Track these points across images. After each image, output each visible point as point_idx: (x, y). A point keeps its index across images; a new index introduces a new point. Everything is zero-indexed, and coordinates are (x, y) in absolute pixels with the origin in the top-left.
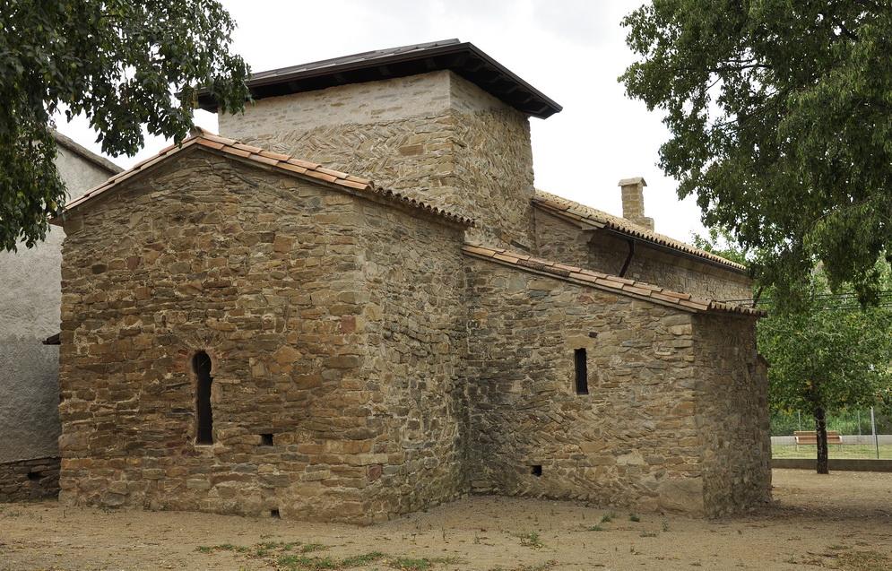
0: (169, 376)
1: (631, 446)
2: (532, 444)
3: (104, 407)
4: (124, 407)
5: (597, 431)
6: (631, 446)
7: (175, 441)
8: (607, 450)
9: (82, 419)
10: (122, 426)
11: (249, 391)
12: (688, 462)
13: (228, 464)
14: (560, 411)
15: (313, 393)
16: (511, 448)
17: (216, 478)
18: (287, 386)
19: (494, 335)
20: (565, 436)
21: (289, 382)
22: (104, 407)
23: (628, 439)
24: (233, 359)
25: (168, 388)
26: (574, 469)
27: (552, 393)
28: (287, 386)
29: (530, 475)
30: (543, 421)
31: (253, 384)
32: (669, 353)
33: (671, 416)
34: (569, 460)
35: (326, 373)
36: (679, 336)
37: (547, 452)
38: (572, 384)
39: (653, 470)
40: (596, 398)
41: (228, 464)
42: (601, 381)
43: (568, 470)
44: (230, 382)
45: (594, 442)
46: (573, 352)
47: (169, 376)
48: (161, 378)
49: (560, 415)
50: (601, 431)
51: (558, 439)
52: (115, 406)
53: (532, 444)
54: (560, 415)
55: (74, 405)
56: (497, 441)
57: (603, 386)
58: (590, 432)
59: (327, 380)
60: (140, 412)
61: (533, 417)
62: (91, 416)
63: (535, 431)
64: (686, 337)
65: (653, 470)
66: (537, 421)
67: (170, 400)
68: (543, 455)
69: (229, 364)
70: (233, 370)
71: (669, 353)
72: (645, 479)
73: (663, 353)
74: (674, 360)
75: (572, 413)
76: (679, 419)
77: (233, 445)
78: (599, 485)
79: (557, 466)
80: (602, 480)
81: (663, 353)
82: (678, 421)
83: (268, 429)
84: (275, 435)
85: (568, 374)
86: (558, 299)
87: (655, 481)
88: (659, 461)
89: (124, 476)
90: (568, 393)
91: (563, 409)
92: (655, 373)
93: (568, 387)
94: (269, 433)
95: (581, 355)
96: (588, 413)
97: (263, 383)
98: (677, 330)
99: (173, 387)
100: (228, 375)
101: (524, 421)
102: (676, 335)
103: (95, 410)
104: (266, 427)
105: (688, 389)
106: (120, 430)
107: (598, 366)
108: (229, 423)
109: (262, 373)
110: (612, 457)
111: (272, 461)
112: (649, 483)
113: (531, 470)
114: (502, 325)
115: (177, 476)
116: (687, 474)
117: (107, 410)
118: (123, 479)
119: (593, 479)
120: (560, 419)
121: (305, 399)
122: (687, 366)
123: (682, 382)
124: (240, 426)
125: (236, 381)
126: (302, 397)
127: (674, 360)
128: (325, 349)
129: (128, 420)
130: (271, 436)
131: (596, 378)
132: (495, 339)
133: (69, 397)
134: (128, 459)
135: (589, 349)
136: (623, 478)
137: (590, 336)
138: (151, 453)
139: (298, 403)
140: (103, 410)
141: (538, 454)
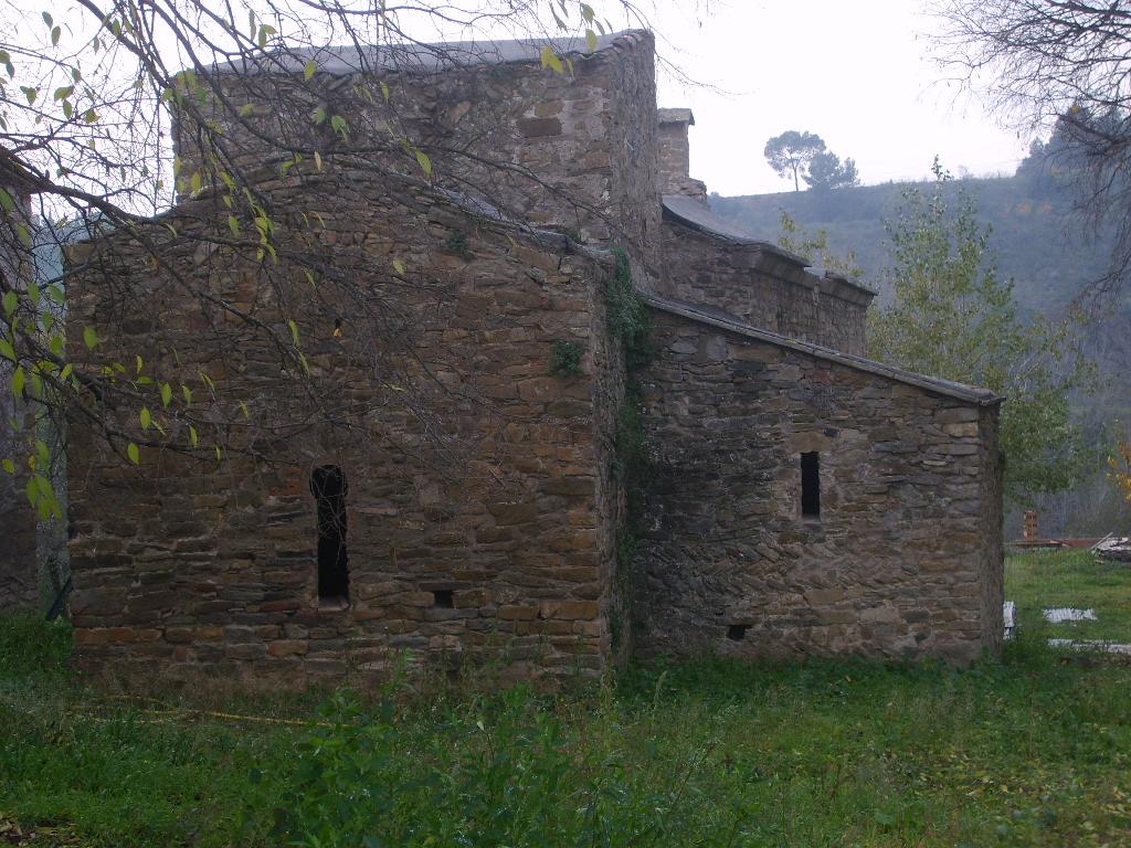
0: (272, 500)
1: (883, 596)
2: (730, 592)
3: (152, 547)
4: (190, 547)
5: (831, 575)
6: (883, 596)
7: (276, 605)
8: (845, 602)
9: (116, 566)
10: (187, 578)
11: (413, 526)
12: (964, 618)
13: (378, 637)
14: (776, 544)
15: (522, 531)
16: (697, 598)
17: (357, 657)
18: (479, 519)
19: (673, 426)
20: (781, 582)
21: (482, 514)
22: (152, 547)
23: (878, 585)
24: (387, 478)
25: (273, 519)
26: (794, 630)
27: (764, 517)
28: (479, 519)
29: (725, 639)
30: (749, 559)
31: (421, 516)
32: (943, 463)
33: (941, 552)
34: (788, 616)
35: (543, 501)
36: (958, 438)
37: (754, 604)
38: (797, 506)
39: (912, 630)
40: (832, 525)
41: (378, 637)
42: (842, 502)
43: (786, 632)
44: (382, 512)
45: (826, 590)
46: (799, 456)
47: (272, 500)
48: (256, 504)
49: (775, 549)
50: (838, 574)
51: (772, 586)
52: (174, 547)
53: (730, 592)
54: (775, 549)
55: (101, 545)
56: (676, 588)
57: (845, 508)
58: (821, 575)
59: (544, 512)
60: (220, 556)
61: (733, 554)
62: (129, 561)
63: (735, 574)
64: (969, 440)
65: (912, 630)
66: (739, 558)
67: (273, 538)
68: (748, 609)
69: (379, 484)
70: (386, 494)
71: (943, 463)
72: (899, 644)
73: (934, 463)
74: (950, 474)
75: (796, 547)
76: (953, 557)
77: (385, 607)
78: (833, 653)
79: (768, 625)
80: (837, 646)
81: (934, 463)
82: (952, 560)
83: (446, 584)
84: (460, 592)
85: (790, 491)
86: (777, 378)
87: (914, 644)
88: (920, 617)
89: (191, 653)
90: (791, 517)
91: (781, 541)
92: (921, 491)
93: (790, 509)
94: (448, 589)
95: (810, 463)
96: (819, 547)
97: (436, 516)
98: (956, 430)
99: (278, 518)
100: (377, 500)
101: (718, 557)
102: (954, 437)
103: (135, 553)
104: (443, 581)
105: (969, 514)
106: (181, 583)
107: (836, 478)
108: (380, 574)
109: (436, 499)
110: (852, 611)
111: (455, 631)
112: (907, 649)
113: (725, 630)
114: (686, 413)
115: (288, 655)
116: (961, 634)
117: (159, 553)
118: (192, 660)
119: (823, 644)
120: (773, 555)
121: (509, 539)
122: (967, 483)
123: (961, 506)
124: (399, 579)
125: (392, 512)
126: (505, 536)
127: (950, 474)
128: (542, 466)
129: (195, 568)
130: (450, 593)
131: (833, 497)
132: (675, 434)
133: (88, 530)
134: (199, 629)
135: (825, 454)
136: (869, 642)
137: (826, 434)
138: (240, 621)
139: (497, 545)
140: (150, 553)
141: (738, 609)
